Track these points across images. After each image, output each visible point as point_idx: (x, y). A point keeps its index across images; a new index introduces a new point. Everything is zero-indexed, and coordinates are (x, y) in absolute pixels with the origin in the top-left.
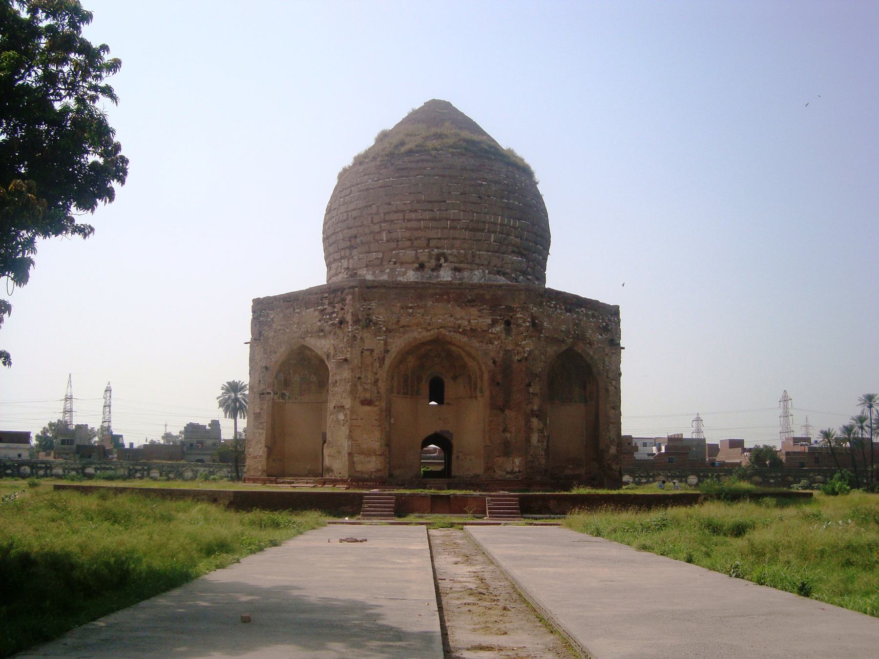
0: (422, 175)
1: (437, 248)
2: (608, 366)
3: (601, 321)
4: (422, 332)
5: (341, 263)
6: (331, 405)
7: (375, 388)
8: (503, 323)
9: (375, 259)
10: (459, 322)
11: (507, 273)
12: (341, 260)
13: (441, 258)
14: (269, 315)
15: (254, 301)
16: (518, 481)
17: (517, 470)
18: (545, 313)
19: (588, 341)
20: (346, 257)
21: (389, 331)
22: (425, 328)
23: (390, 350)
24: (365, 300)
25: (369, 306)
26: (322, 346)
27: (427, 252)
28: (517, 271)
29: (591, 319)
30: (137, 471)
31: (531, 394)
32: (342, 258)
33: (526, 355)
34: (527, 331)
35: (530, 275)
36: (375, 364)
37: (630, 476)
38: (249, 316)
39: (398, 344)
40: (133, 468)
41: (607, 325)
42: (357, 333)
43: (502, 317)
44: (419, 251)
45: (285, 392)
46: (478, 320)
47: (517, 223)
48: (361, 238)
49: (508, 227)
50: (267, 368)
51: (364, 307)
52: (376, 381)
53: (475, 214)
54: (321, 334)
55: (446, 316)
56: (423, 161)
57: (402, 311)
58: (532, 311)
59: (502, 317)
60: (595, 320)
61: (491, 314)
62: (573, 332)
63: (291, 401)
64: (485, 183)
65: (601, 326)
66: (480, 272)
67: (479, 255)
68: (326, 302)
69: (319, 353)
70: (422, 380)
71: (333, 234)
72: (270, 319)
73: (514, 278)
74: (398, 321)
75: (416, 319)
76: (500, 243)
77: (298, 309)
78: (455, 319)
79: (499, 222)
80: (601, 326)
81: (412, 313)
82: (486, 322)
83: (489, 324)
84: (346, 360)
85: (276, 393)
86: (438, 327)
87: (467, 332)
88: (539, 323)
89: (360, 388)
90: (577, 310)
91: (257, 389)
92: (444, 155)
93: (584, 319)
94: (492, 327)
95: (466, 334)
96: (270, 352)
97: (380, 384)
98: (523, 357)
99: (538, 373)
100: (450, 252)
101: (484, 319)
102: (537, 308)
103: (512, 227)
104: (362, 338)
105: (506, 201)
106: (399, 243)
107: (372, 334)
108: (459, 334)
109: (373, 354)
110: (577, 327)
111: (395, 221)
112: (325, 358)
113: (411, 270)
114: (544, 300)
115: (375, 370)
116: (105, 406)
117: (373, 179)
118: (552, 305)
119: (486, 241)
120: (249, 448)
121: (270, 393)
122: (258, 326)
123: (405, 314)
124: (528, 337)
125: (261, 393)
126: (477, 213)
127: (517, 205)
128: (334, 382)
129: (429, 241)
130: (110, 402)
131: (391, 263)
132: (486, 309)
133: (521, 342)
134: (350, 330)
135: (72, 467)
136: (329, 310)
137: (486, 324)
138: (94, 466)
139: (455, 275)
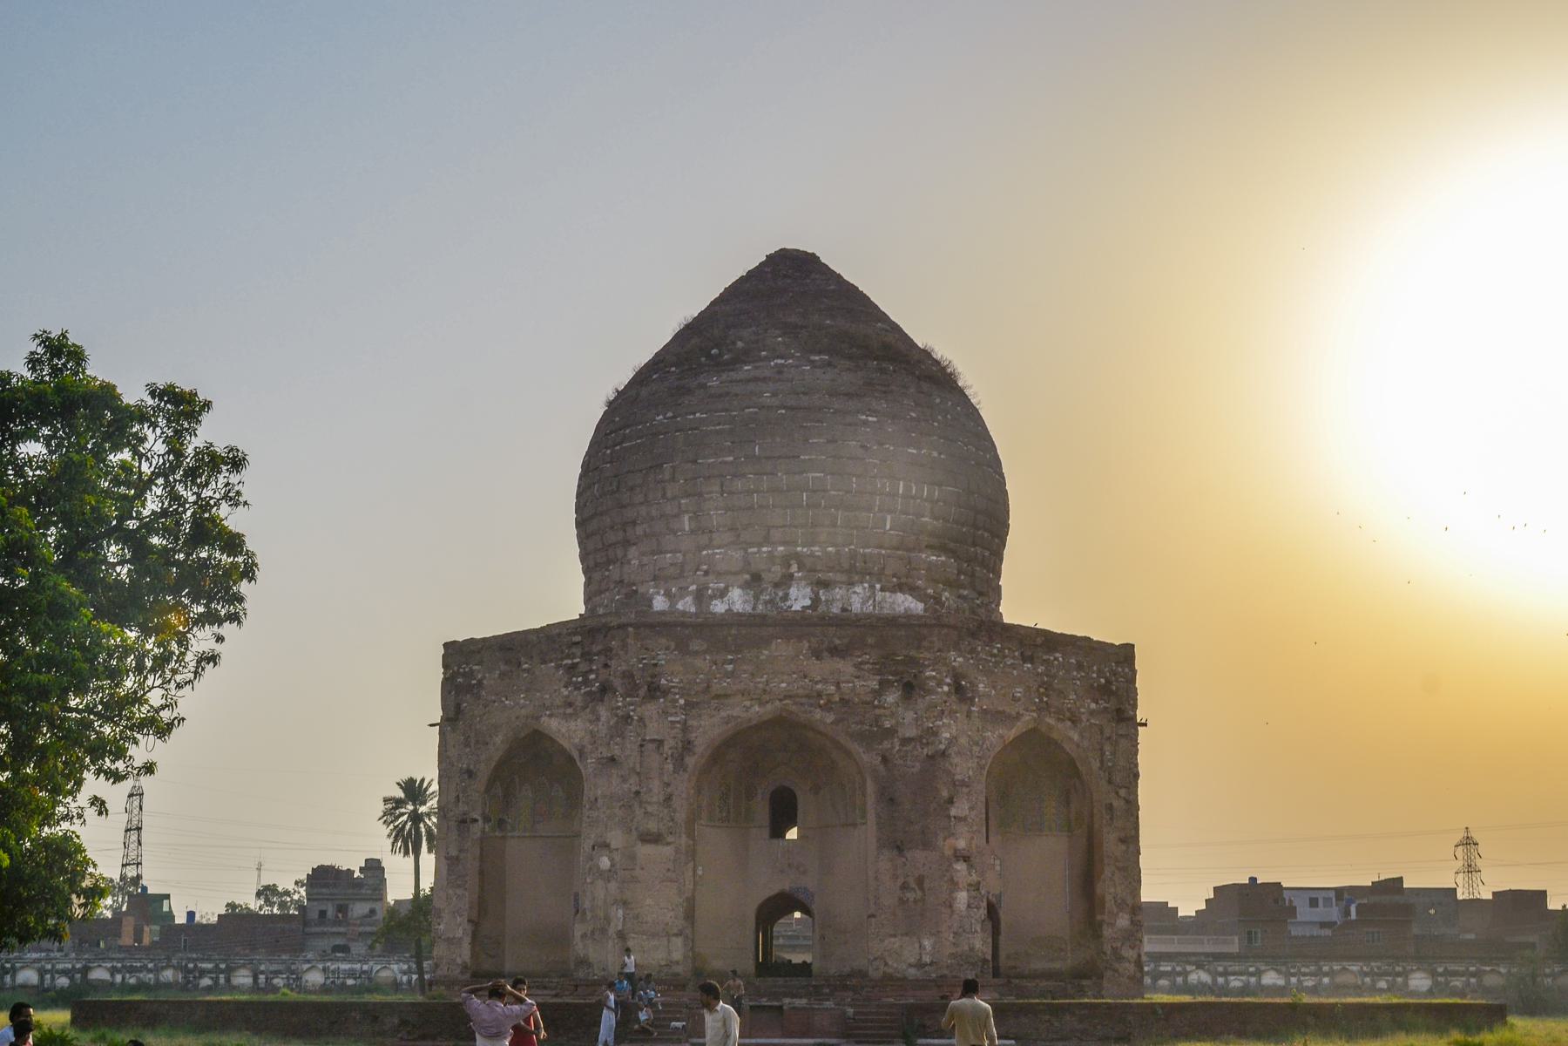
0: (755, 407)
1: (784, 543)
2: (1109, 760)
3: (1095, 675)
4: (752, 706)
5: (609, 570)
6: (587, 845)
7: (666, 811)
8: (901, 687)
9: (671, 565)
10: (819, 686)
11: (918, 588)
12: (610, 565)
13: (792, 562)
14: (475, 674)
15: (444, 645)
16: (930, 981)
17: (928, 961)
18: (981, 667)
19: (1068, 714)
20: (617, 560)
21: (689, 705)
22: (756, 699)
23: (693, 741)
24: (646, 649)
25: (654, 659)
26: (568, 731)
27: (765, 553)
28: (939, 583)
29: (1075, 673)
30: (203, 973)
31: (953, 819)
32: (609, 562)
33: (942, 747)
34: (945, 702)
35: (965, 589)
36: (666, 766)
37: (1279, 972)
38: (438, 674)
39: (709, 729)
40: (196, 966)
41: (1108, 682)
42: (632, 711)
43: (898, 678)
44: (750, 550)
45: (505, 817)
46: (853, 682)
47: (937, 493)
48: (644, 526)
49: (919, 501)
50: (470, 774)
51: (644, 661)
52: (668, 798)
53: (854, 479)
54: (569, 711)
55: (795, 676)
56: (756, 379)
57: (714, 667)
58: (954, 664)
59: (898, 678)
60: (1083, 674)
61: (879, 672)
62: (1037, 700)
63: (516, 834)
64: (875, 419)
65: (1095, 685)
66: (865, 588)
67: (864, 555)
68: (577, 651)
69: (566, 745)
70: (756, 794)
71: (592, 517)
72: (474, 682)
73: (931, 597)
74: (708, 687)
75: (741, 682)
76: (904, 532)
77: (526, 663)
78: (810, 681)
79: (901, 492)
80: (1095, 685)
81: (733, 672)
82: (868, 686)
83: (874, 691)
84: (612, 759)
85: (487, 819)
86: (779, 697)
87: (833, 706)
88: (968, 685)
89: (639, 812)
90: (1045, 657)
91: (452, 814)
92: (797, 367)
93: (1061, 673)
94: (881, 695)
95: (832, 708)
96: (477, 742)
97: (677, 802)
98: (936, 752)
99: (966, 780)
100: (809, 553)
101: (864, 681)
102: (964, 657)
103: (926, 500)
104: (641, 719)
105: (915, 451)
106: (714, 535)
107: (660, 711)
108: (818, 710)
109: (661, 748)
110: (1046, 689)
111: (706, 496)
112: (575, 755)
113: (735, 588)
114: (980, 643)
115: (666, 779)
116: (127, 830)
117: (666, 414)
118: (995, 651)
119: (876, 528)
120: (439, 924)
121: (475, 821)
122: (453, 693)
123: (720, 673)
124: (946, 713)
125: (460, 819)
126: (858, 477)
127: (934, 457)
128: (592, 799)
129: (769, 531)
130: (140, 821)
131: (698, 573)
132: (868, 663)
133: (933, 723)
134: (620, 704)
135: (60, 967)
136: (583, 667)
137: (869, 690)
138: (109, 965)
139: (817, 594)
